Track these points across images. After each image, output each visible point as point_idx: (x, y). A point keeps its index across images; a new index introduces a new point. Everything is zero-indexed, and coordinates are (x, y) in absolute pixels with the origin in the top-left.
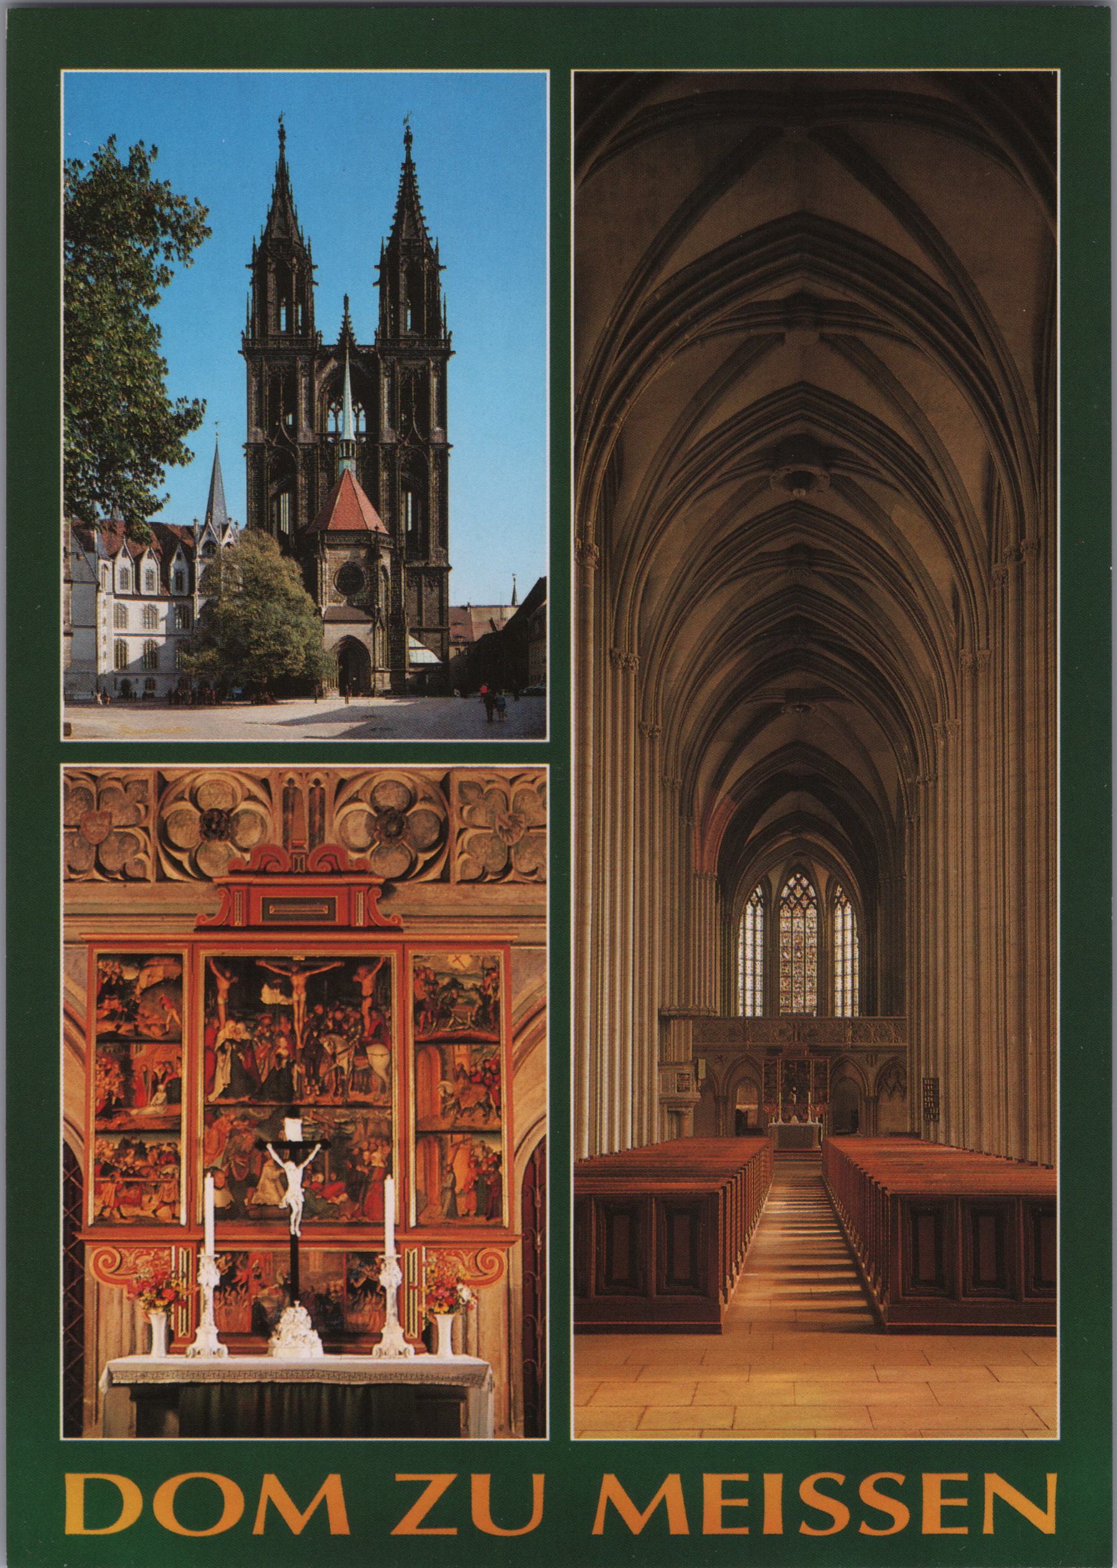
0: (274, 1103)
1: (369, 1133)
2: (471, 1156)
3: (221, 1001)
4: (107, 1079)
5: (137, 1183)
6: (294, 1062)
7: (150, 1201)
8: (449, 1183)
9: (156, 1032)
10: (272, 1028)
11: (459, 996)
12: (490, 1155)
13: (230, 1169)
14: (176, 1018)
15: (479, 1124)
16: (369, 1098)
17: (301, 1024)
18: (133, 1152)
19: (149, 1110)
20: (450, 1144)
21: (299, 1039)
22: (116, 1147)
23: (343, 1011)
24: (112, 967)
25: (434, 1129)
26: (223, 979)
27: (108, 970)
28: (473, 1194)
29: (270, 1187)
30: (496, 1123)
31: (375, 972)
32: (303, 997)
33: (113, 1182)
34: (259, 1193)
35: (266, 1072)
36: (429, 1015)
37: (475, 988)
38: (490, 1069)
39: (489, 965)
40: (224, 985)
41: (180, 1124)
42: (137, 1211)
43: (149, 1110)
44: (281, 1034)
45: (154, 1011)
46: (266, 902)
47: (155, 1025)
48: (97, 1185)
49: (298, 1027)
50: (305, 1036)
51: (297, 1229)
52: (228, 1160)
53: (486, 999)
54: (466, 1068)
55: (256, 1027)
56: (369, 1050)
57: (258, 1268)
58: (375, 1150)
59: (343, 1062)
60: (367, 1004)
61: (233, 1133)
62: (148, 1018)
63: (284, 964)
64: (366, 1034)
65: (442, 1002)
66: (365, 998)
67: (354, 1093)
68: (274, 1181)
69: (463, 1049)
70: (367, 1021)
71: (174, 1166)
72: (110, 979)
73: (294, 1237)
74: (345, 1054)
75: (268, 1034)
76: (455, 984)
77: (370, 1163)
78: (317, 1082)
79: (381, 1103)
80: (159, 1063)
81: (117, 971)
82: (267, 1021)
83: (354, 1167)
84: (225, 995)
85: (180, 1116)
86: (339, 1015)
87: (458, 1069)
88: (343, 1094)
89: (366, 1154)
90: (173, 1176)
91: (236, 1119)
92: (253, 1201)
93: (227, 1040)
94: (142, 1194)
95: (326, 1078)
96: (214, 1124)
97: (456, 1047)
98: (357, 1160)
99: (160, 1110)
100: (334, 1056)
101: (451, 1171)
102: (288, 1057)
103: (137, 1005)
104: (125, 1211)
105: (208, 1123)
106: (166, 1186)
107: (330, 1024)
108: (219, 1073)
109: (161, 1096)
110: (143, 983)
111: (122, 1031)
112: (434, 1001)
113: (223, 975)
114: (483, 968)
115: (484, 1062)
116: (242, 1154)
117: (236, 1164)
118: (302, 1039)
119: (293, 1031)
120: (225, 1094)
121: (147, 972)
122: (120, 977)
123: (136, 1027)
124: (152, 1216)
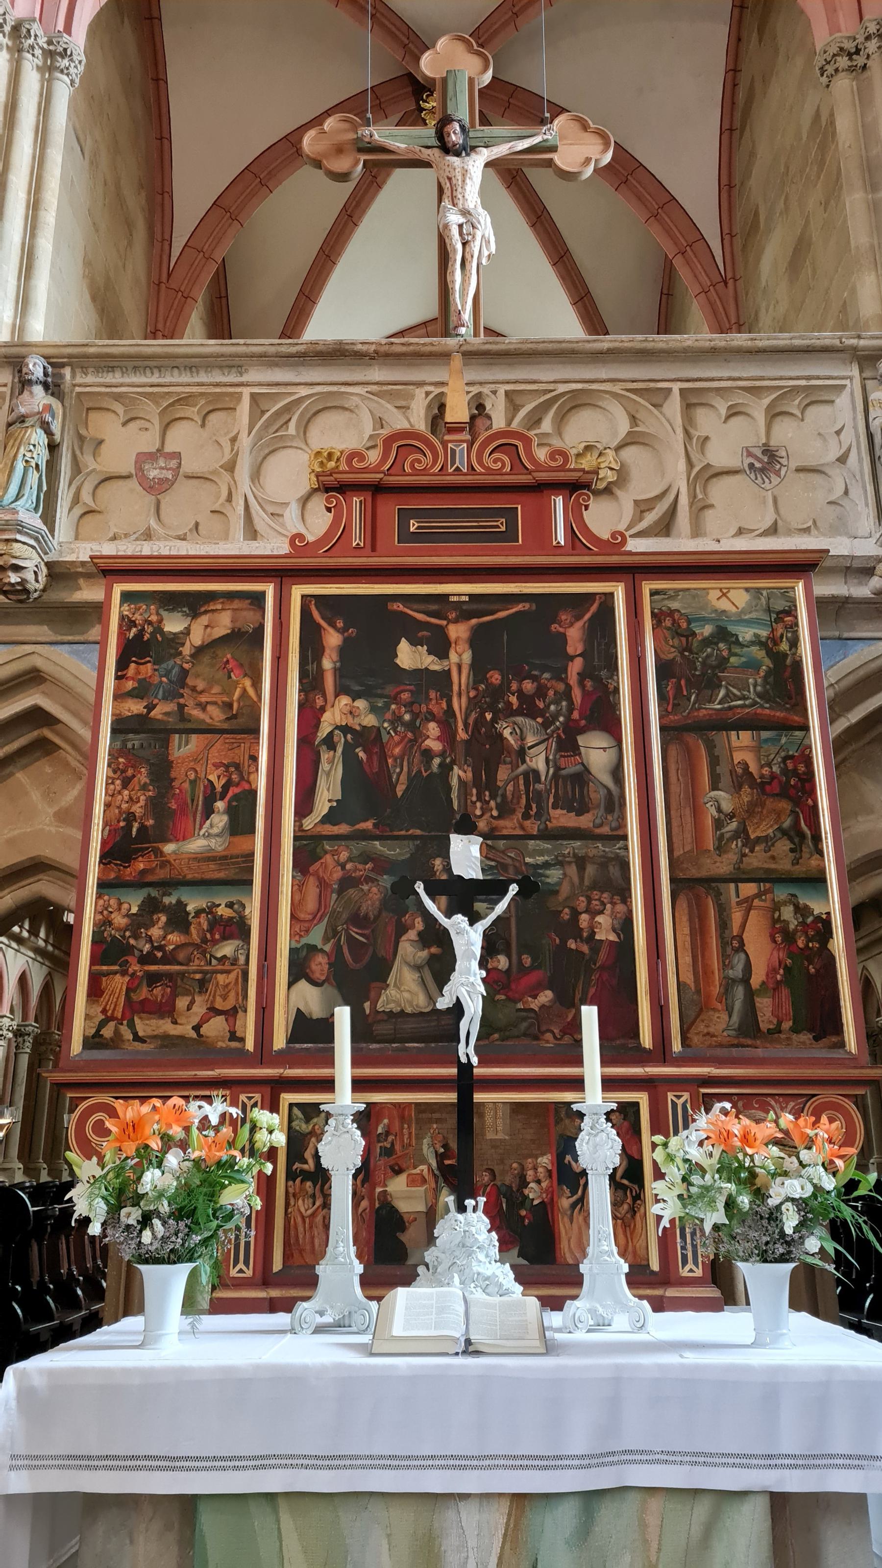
0: (418, 832)
1: (587, 882)
2: (775, 921)
3: (327, 664)
4: (126, 792)
5: (170, 976)
6: (453, 762)
7: (189, 1008)
8: (737, 972)
9: (215, 715)
10: (416, 708)
11: (732, 654)
12: (810, 920)
13: (338, 947)
14: (251, 692)
15: (785, 865)
16: (585, 821)
17: (464, 700)
18: (164, 919)
19: (196, 845)
20: (734, 899)
21: (460, 725)
22: (134, 910)
23: (534, 679)
24: (143, 614)
25: (704, 873)
26: (331, 630)
27: (138, 618)
28: (785, 992)
29: (410, 978)
30: (814, 862)
31: (587, 616)
32: (467, 657)
33: (124, 973)
34: (392, 992)
35: (403, 778)
36: (683, 682)
37: (757, 641)
38: (795, 770)
39: (780, 605)
40: (333, 639)
41: (251, 870)
42: (165, 1026)
43: (196, 845)
44: (431, 717)
45: (211, 682)
46: (405, 515)
47: (215, 703)
48: (95, 981)
49: (459, 705)
50: (471, 721)
51: (471, 1050)
52: (335, 933)
53: (778, 658)
54: (753, 768)
55: (387, 706)
56: (581, 740)
57: (387, 1133)
58: (601, 912)
59: (538, 761)
60: (576, 667)
61: (347, 883)
62: (201, 692)
63: (434, 607)
64: (576, 715)
65: (704, 663)
66: (572, 658)
67: (559, 811)
68: (418, 968)
69: (745, 737)
70: (577, 694)
71: (237, 942)
72: (141, 632)
73: (466, 1069)
74: (542, 747)
75: (407, 717)
76: (722, 634)
77: (594, 933)
78: (493, 797)
79: (605, 830)
80: (216, 766)
81: (154, 618)
82: (405, 696)
83: (564, 942)
84: (335, 657)
85: (252, 854)
86: (528, 686)
87: (739, 771)
88: (538, 816)
89: (584, 917)
90: (234, 961)
91: (350, 859)
92: (380, 1007)
93: (337, 727)
94: (174, 996)
95: (510, 788)
96: (312, 869)
97: (733, 733)
98: (572, 929)
99: (217, 845)
100: (522, 753)
101: (741, 948)
102: (442, 754)
103: (184, 673)
104: (144, 1026)
105: (301, 864)
106: (221, 978)
107: (514, 700)
108: (322, 783)
109: (219, 820)
110: (197, 637)
111: (156, 713)
112: (691, 664)
113: (333, 625)
114: (769, 610)
115: (785, 759)
116: (358, 920)
117: (350, 939)
118: (466, 725)
119: (450, 712)
120: (330, 818)
121: (204, 620)
122: (159, 630)
123: (181, 707)
124: (194, 1035)
